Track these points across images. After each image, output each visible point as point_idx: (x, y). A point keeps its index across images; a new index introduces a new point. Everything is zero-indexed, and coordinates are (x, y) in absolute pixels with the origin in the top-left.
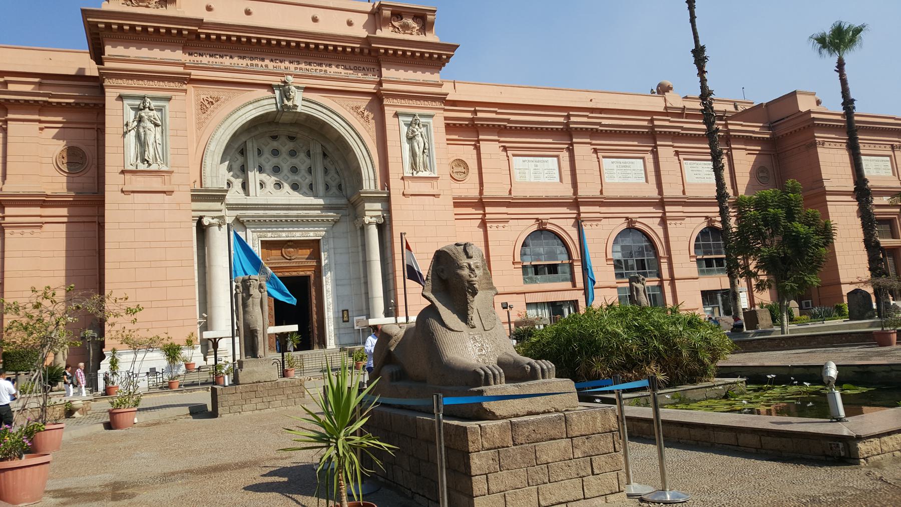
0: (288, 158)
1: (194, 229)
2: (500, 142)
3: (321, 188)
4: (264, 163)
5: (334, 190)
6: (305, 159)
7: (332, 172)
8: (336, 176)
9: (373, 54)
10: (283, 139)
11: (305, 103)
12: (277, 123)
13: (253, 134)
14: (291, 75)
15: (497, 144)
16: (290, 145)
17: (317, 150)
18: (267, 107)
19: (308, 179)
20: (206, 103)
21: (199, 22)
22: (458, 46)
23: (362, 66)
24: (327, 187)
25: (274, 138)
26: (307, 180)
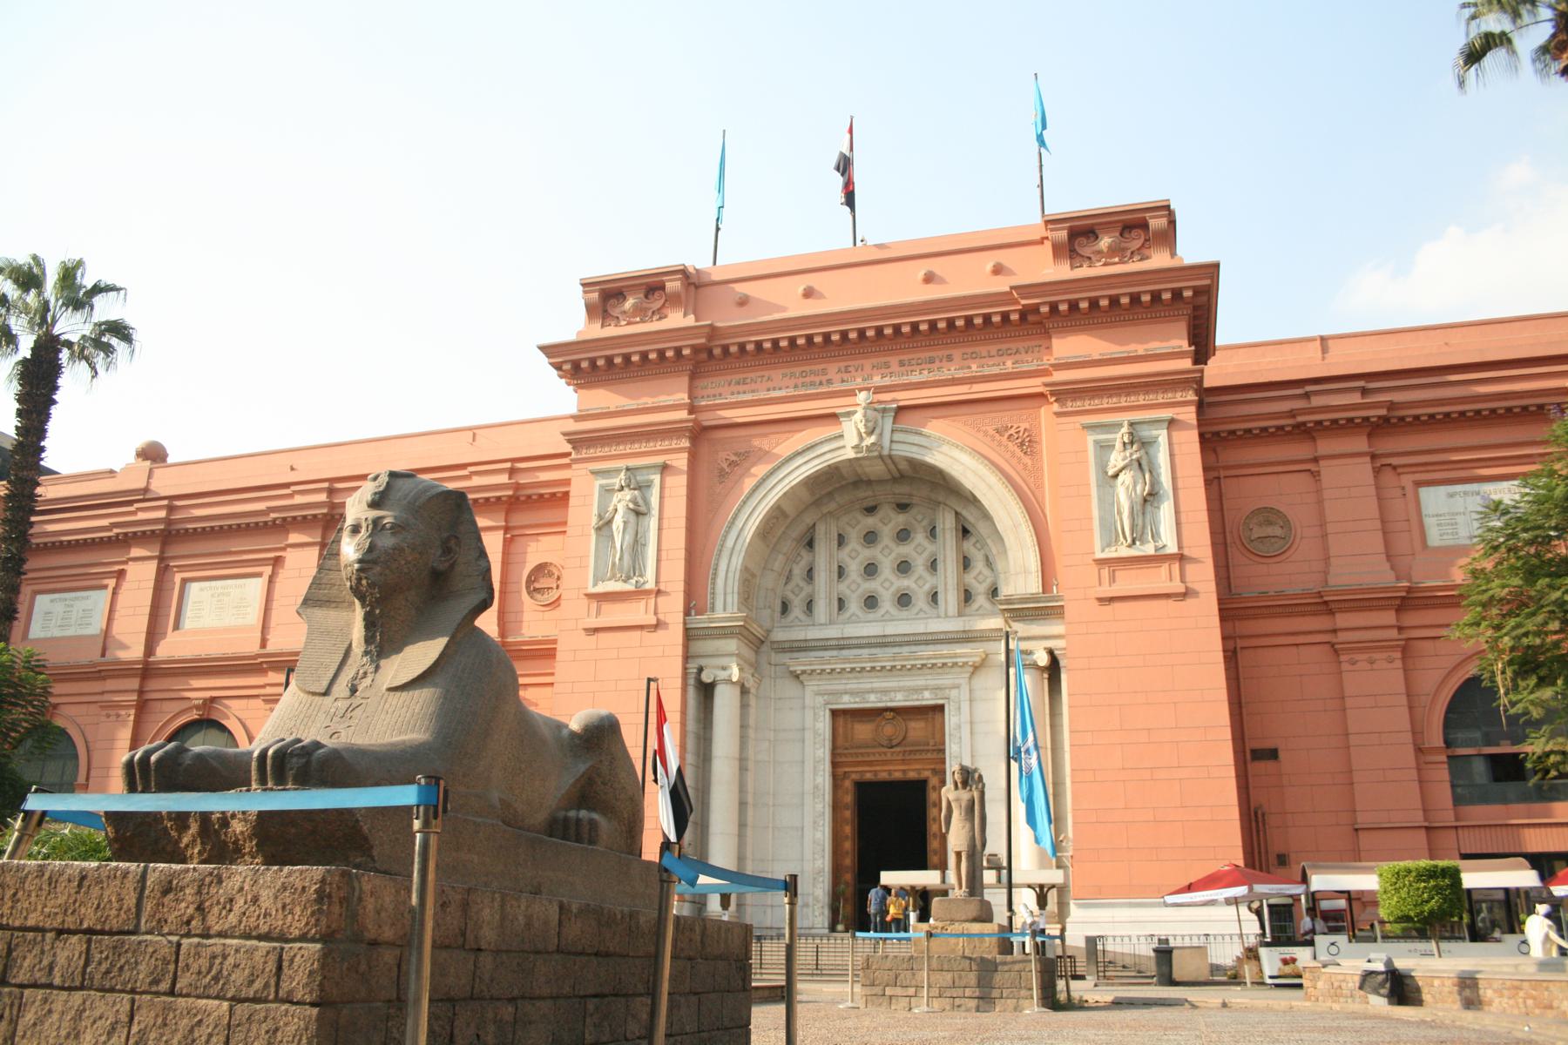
0: (892, 545)
1: (691, 692)
2: (1374, 457)
3: (950, 599)
4: (847, 559)
6: (926, 543)
8: (986, 572)
9: (1031, 318)
10: (886, 511)
11: (897, 437)
12: (869, 482)
13: (825, 510)
14: (868, 389)
15: (1364, 468)
16: (900, 520)
17: (947, 523)
18: (828, 456)
19: (929, 582)
20: (725, 466)
21: (713, 332)
23: (1014, 346)
24: (967, 596)
25: (871, 510)
26: (927, 587)
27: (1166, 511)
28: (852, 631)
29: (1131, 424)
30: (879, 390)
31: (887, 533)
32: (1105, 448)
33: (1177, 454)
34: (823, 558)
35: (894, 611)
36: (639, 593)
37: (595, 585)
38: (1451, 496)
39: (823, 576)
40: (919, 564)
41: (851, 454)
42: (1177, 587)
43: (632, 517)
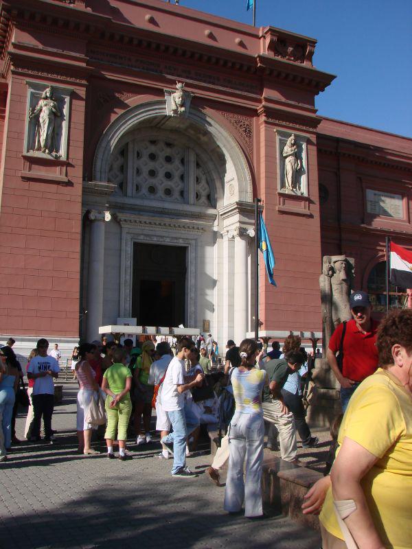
0: (164, 163)
5: (203, 199)
6: (180, 166)
7: (203, 182)
8: (206, 186)
14: (183, 83)
16: (168, 152)
19: (181, 185)
22: (333, 77)
24: (198, 196)
25: (153, 142)
27: (304, 179)
28: (147, 203)
29: (295, 136)
30: (187, 85)
31: (162, 156)
32: (283, 144)
33: (308, 155)
34: (132, 163)
35: (163, 196)
36: (56, 163)
37: (28, 151)
38: (375, 194)
39: (131, 172)
40: (177, 175)
41: (172, 114)
42: (307, 212)
43: (53, 118)
